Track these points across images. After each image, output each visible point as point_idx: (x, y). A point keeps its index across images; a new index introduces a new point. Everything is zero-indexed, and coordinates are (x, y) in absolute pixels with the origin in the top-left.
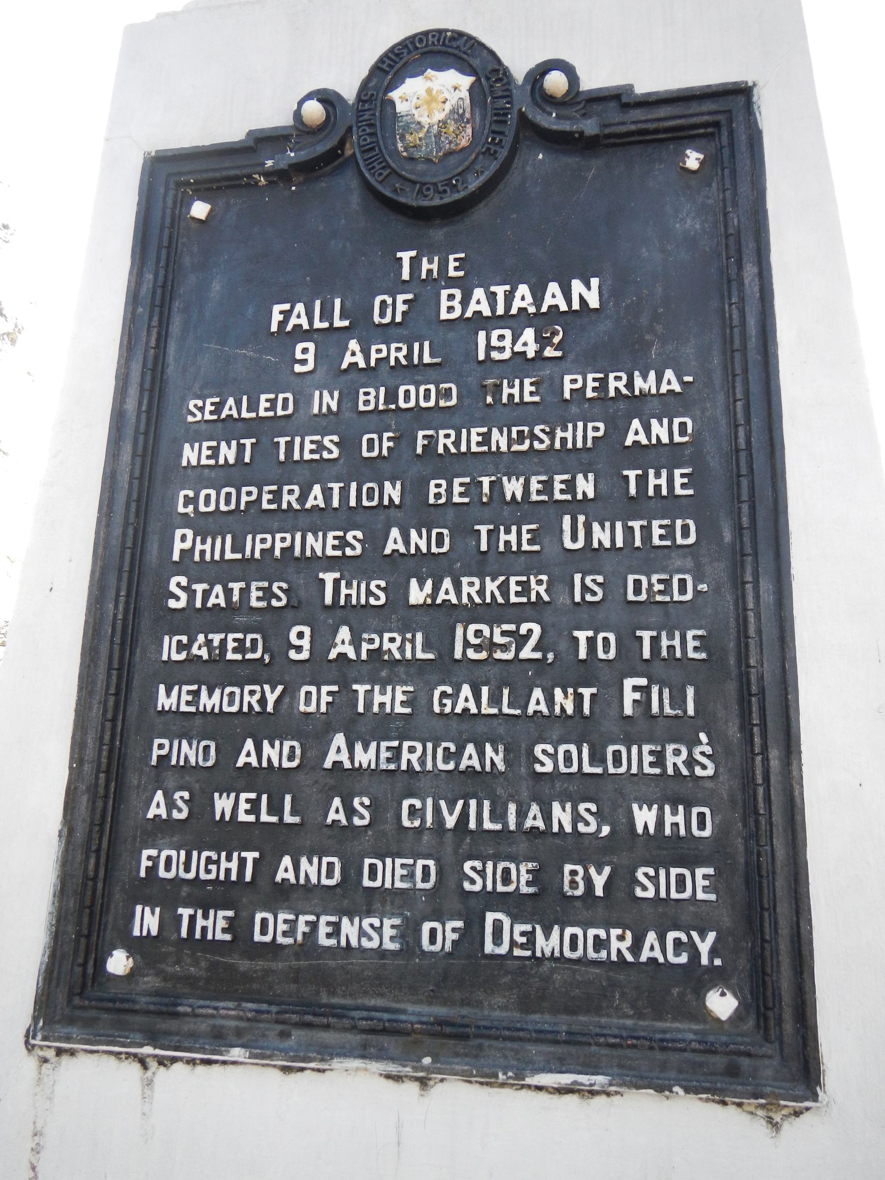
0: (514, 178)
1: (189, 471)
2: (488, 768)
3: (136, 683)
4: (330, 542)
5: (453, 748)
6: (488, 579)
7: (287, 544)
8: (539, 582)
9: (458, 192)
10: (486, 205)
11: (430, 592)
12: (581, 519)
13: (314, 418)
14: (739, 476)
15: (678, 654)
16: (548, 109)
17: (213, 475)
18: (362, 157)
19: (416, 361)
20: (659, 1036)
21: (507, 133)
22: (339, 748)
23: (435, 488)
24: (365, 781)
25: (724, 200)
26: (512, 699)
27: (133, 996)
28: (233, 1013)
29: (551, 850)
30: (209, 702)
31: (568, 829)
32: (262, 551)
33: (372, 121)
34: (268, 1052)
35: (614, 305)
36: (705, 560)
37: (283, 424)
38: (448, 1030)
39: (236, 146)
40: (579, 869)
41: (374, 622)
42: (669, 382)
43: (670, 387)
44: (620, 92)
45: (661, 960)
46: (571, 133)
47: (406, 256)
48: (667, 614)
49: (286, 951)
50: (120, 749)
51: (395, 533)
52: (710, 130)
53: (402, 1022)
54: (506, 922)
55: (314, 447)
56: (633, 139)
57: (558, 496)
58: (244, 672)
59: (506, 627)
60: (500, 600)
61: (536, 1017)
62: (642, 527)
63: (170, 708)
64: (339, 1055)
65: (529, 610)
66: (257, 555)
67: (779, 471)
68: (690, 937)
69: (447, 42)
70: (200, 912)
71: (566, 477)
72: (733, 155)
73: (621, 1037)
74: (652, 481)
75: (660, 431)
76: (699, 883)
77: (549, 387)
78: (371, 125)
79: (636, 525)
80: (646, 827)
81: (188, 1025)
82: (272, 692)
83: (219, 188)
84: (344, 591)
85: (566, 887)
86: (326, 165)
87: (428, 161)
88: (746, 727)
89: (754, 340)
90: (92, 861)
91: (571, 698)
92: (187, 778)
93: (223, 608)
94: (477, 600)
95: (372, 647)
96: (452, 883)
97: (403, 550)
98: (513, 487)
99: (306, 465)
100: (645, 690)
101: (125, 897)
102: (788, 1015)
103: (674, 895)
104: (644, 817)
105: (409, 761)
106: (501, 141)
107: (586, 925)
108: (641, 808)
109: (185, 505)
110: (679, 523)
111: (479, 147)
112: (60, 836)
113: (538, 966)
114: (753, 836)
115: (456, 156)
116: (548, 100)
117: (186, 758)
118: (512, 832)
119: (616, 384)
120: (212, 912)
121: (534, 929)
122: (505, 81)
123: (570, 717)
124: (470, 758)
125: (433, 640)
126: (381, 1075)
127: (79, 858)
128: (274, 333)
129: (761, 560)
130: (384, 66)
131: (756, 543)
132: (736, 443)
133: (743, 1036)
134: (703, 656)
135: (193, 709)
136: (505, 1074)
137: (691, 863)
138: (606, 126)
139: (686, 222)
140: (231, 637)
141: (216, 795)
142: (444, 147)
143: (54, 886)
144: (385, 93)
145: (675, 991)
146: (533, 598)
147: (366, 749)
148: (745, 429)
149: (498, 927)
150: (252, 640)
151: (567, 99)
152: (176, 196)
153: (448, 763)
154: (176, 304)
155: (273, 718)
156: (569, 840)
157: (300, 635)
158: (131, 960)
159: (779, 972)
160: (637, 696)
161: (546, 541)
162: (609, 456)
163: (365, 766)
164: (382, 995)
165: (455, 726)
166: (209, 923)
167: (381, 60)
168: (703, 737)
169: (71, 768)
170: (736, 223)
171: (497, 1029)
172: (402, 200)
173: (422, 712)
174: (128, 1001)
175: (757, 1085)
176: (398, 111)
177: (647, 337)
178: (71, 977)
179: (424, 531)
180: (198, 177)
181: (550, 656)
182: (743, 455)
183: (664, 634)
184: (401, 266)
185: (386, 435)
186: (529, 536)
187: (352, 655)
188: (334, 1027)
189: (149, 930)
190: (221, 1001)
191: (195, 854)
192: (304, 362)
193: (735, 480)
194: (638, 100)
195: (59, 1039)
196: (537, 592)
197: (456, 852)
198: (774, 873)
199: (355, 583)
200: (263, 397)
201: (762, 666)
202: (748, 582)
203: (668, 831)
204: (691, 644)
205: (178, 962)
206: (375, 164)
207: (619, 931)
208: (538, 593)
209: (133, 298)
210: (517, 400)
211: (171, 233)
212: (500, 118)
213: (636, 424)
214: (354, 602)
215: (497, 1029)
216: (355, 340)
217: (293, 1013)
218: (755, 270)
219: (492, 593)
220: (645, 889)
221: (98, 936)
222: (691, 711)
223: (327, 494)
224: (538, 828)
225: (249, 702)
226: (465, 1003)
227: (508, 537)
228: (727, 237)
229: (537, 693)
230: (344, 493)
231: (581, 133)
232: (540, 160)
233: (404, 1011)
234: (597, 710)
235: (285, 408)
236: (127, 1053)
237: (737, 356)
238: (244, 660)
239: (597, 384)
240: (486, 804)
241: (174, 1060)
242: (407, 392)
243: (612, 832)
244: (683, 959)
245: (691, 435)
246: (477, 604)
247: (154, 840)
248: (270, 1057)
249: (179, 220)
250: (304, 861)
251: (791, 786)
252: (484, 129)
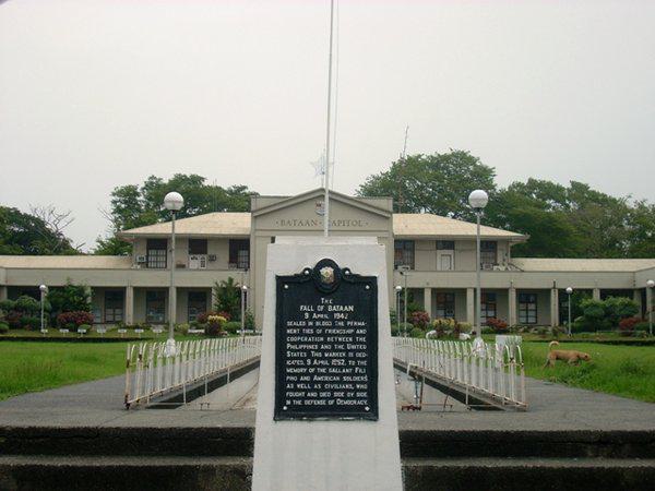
29: (346, 391)
76: (365, 394)
162: (354, 335)
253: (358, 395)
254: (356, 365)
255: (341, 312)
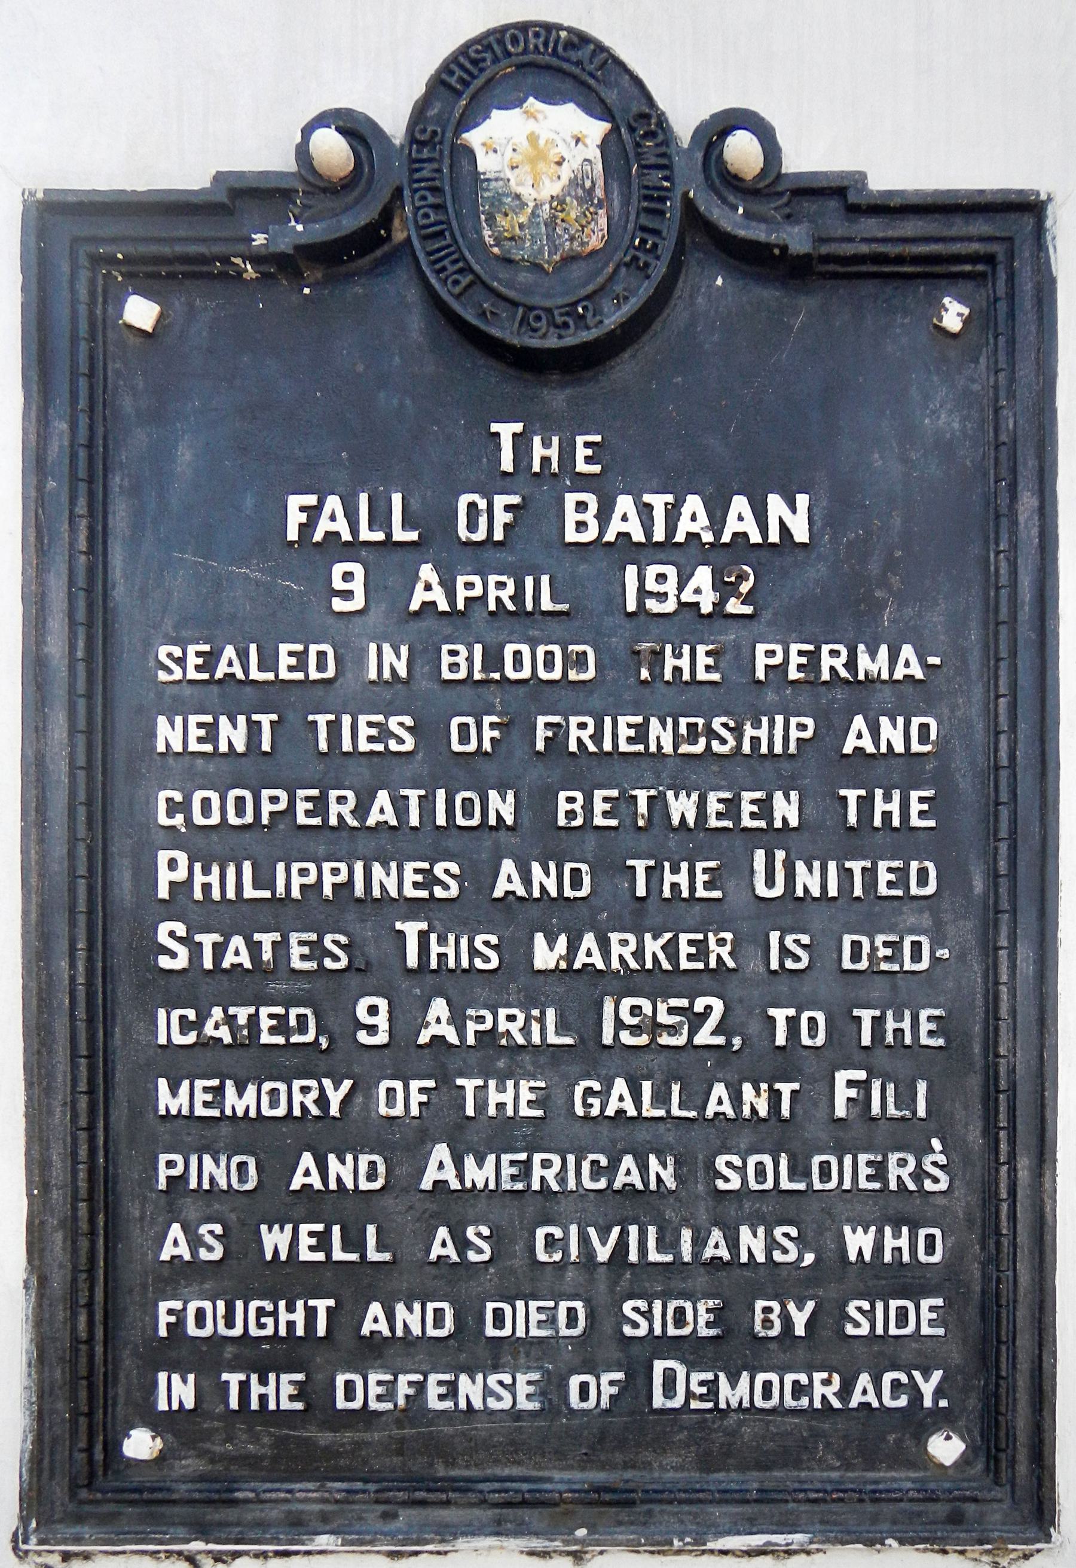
0: (677, 314)
1: (170, 760)
2: (653, 1186)
3: (119, 1077)
4: (410, 877)
5: (604, 1162)
6: (648, 936)
7: (343, 877)
8: (721, 942)
9: (588, 328)
10: (633, 356)
11: (564, 952)
12: (780, 855)
13: (370, 687)
14: (997, 804)
15: (908, 1040)
16: (731, 198)
17: (211, 768)
18: (424, 248)
19: (529, 606)
20: (869, 1487)
21: (664, 234)
22: (441, 1163)
23: (566, 804)
24: (482, 1205)
25: (996, 387)
26: (684, 1098)
27: (168, 1484)
28: (315, 1495)
29: (736, 1284)
30: (240, 1102)
31: (761, 1258)
32: (303, 887)
33: (437, 183)
34: (368, 1537)
35: (831, 539)
36: (946, 917)
37: (321, 693)
38: (607, 1497)
39: (195, 200)
40: (775, 1305)
41: (483, 994)
42: (907, 664)
43: (908, 672)
44: (846, 183)
45: (875, 1404)
46: (768, 247)
47: (507, 431)
48: (894, 988)
49: (384, 1418)
50: (106, 1168)
51: (508, 866)
52: (980, 268)
53: (546, 1491)
54: (681, 1370)
55: (373, 732)
56: (864, 268)
57: (747, 822)
58: (290, 1061)
59: (674, 1002)
60: (666, 965)
61: (721, 1476)
62: (864, 869)
63: (180, 1111)
64: (464, 1534)
65: (705, 978)
66: (296, 893)
67: (1050, 799)
68: (911, 1377)
69: (560, 49)
70: (254, 1378)
71: (758, 795)
72: (1011, 315)
73: (825, 1491)
74: (880, 806)
75: (892, 734)
76: (925, 1316)
77: (733, 658)
78: (435, 190)
79: (856, 866)
80: (860, 1253)
81: (252, 1514)
82: (336, 1089)
83: (171, 276)
84: (435, 949)
85: (758, 1327)
86: (361, 255)
87: (537, 267)
88: (990, 1131)
89: (1027, 608)
90: (83, 1319)
91: (765, 1095)
92: (217, 1206)
93: (248, 970)
94: (633, 965)
95: (481, 1027)
96: (607, 1328)
97: (521, 892)
98: (682, 807)
99: (364, 760)
100: (864, 1086)
101: (140, 1363)
102: (1023, 1456)
103: (893, 1331)
104: (859, 1242)
105: (542, 1178)
106: (655, 246)
107: (782, 1370)
108: (854, 1231)
109: (170, 814)
110: (914, 865)
111: (620, 254)
112: (26, 1287)
113: (722, 1419)
114: (992, 1260)
115: (582, 264)
116: (730, 182)
117: (212, 1179)
118: (687, 1264)
119: (832, 661)
120: (272, 1377)
121: (717, 1377)
122: (660, 138)
123: (764, 1120)
124: (628, 1172)
125: (571, 1019)
126: (522, 1552)
127: (61, 1315)
128: (292, 543)
129: (1020, 919)
130: (453, 81)
131: (1015, 896)
132: (996, 757)
133: (970, 1481)
134: (941, 1042)
135: (215, 1113)
136: (681, 1540)
137: (915, 1294)
138: (823, 240)
139: (939, 418)
140: (264, 1011)
141: (264, 1228)
142: (562, 245)
143: (27, 1352)
144: (457, 133)
145: (891, 1438)
146: (713, 964)
147: (480, 1163)
148: (1009, 738)
149: (669, 1379)
150: (298, 1016)
151: (761, 185)
152: (92, 282)
153: (598, 1180)
154: (116, 480)
155: (339, 1124)
156: (762, 1271)
157: (373, 1010)
158: (158, 1440)
159: (1014, 1410)
160: (853, 1093)
161: (731, 885)
162: (821, 766)
163: (480, 1185)
164: (519, 1463)
165: (605, 1133)
166: (271, 1390)
167: (446, 68)
168: (936, 1144)
169: (30, 1195)
170: (1011, 426)
171: (671, 1492)
172: (495, 332)
173: (559, 1115)
174: (161, 1490)
175: (983, 1531)
176: (480, 169)
177: (878, 594)
178: (71, 1466)
179: (552, 866)
180: (131, 249)
181: (737, 1042)
182: (1004, 774)
183: (890, 1014)
184: (499, 448)
185: (487, 720)
186: (706, 877)
187: (453, 1038)
188: (456, 1503)
189: (181, 1403)
190: (297, 1482)
191: (239, 1305)
192: (347, 595)
193: (992, 809)
194: (873, 201)
195: (65, 1542)
196: (718, 955)
197: (612, 1291)
198: (1015, 1301)
199: (451, 938)
200: (284, 648)
201: (1015, 1055)
202: (1002, 948)
203: (888, 1258)
204: (925, 1027)
205: (229, 1439)
206: (446, 262)
207: (825, 1375)
208: (719, 956)
209: (36, 463)
210: (686, 676)
211: (91, 350)
212: (653, 205)
213: (859, 722)
214: (451, 964)
215: (671, 1492)
216: (430, 566)
217: (399, 1490)
218: (1035, 502)
219: (654, 955)
220: (857, 1325)
221: (105, 1414)
222: (921, 1112)
223: (400, 805)
224: (721, 1258)
225: (302, 1103)
226: (626, 1466)
227: (675, 879)
228: (997, 447)
229: (719, 1090)
230: (427, 804)
231: (784, 248)
232: (719, 288)
233: (549, 1480)
234: (800, 1111)
235: (321, 666)
236: (167, 1551)
237: (1003, 630)
238: (288, 1045)
239: (804, 660)
240: (652, 1230)
241: (236, 1555)
242: (517, 654)
243: (817, 1261)
244: (903, 1402)
245: (936, 743)
246: (632, 971)
247: (175, 1289)
248: (371, 1543)
249: (105, 328)
250: (400, 1309)
251: (1042, 1200)
252: (627, 222)
253: (860, 1320)
254: (842, 1048)
255: (684, 554)
